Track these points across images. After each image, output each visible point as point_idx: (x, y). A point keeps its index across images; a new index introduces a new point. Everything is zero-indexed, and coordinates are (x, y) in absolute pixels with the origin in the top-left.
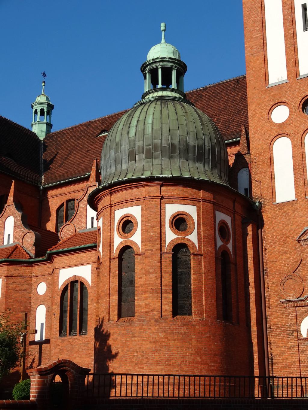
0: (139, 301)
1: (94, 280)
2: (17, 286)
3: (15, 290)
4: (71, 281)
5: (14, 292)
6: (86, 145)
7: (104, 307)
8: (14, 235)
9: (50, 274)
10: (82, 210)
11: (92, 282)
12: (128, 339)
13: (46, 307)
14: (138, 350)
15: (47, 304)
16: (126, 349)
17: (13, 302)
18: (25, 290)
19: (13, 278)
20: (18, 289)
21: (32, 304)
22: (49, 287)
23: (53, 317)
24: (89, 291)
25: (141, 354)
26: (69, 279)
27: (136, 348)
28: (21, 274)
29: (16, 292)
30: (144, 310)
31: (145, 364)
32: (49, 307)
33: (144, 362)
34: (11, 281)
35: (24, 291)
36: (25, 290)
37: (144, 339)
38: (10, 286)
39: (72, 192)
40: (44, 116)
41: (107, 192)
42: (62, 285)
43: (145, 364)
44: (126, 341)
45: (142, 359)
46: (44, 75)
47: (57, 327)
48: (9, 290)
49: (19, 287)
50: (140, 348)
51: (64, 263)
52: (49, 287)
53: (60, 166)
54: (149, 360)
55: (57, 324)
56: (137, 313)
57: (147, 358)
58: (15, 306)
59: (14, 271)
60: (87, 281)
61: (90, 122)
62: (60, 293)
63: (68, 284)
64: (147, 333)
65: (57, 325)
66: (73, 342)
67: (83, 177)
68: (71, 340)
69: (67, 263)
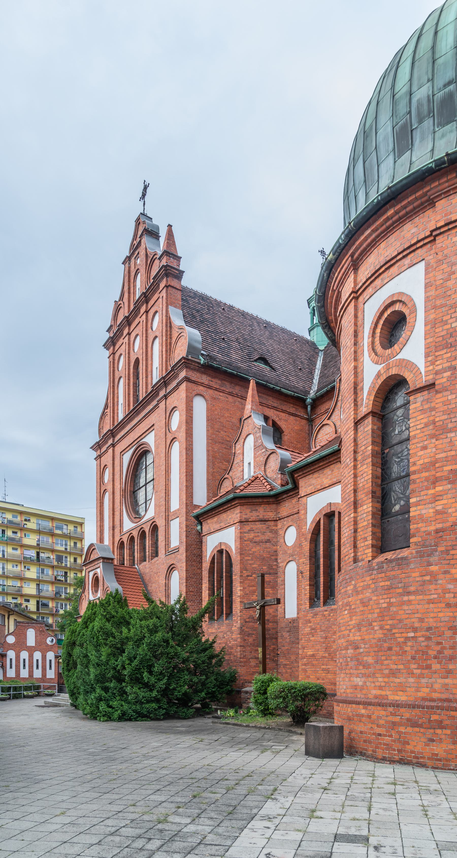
0: (419, 507)
2: (257, 534)
3: (254, 541)
4: (324, 513)
7: (347, 534)
12: (393, 600)
14: (416, 625)
16: (390, 622)
17: (252, 559)
18: (268, 540)
19: (250, 523)
21: (279, 561)
25: (423, 636)
27: (413, 620)
28: (261, 517)
29: (255, 544)
30: (432, 528)
31: (435, 657)
33: (432, 653)
34: (247, 528)
35: (266, 542)
36: (268, 541)
37: (432, 597)
38: (245, 537)
42: (312, 522)
43: (435, 657)
44: (390, 604)
45: (428, 647)
48: (245, 542)
50: (421, 620)
51: (314, 484)
54: (444, 648)
56: (414, 536)
57: (441, 643)
58: (254, 566)
59: (250, 512)
62: (309, 536)
64: (440, 582)
69: (318, 485)
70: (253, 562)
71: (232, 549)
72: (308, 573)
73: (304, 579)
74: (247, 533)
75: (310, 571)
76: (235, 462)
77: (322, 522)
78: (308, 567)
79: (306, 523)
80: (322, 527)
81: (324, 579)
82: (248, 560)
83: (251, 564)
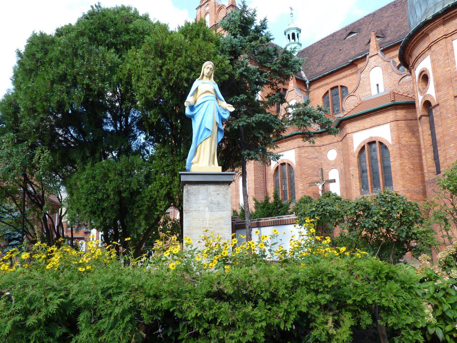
1: (395, 138)
7: (453, 153)
10: (365, 80)
11: (392, 141)
17: (307, 168)
19: (305, 148)
20: (310, 157)
23: (352, 177)
24: (390, 149)
34: (303, 150)
36: (316, 158)
39: (335, 81)
41: (438, 23)
46: (291, 9)
49: (310, 155)
53: (318, 66)
60: (386, 141)
62: (357, 155)
65: (356, 185)
67: (345, 65)
75: (359, 174)
78: (357, 172)
79: (353, 148)
83: (307, 171)
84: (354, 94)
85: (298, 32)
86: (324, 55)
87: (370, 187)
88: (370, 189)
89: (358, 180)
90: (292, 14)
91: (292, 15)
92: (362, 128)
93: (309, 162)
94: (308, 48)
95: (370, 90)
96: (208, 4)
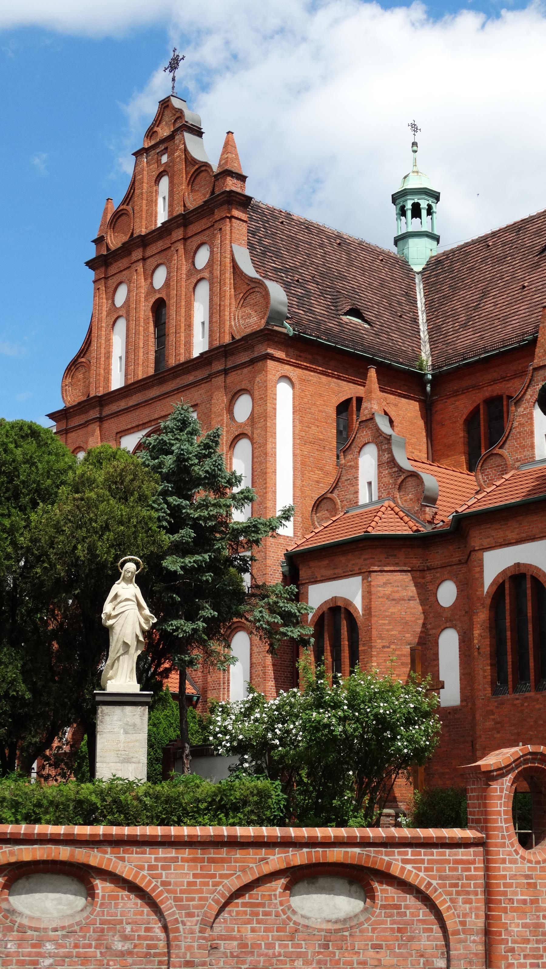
4: (509, 574)
5: (389, 602)
6: (519, 274)
8: (379, 482)
9: (463, 561)
10: (523, 420)
13: (458, 632)
15: (460, 625)
17: (389, 624)
18: (411, 597)
20: (396, 596)
22: (462, 591)
26: (504, 571)
29: (394, 602)
32: (465, 633)
35: (409, 600)
40: (421, 218)
42: (492, 585)
46: (414, 128)
47: (486, 674)
49: (397, 592)
51: (493, 536)
52: (462, 591)
53: (464, 326)
55: (485, 668)
58: (392, 633)
59: (386, 558)
61: (524, 223)
62: (488, 601)
63: (503, 584)
65: (485, 671)
66: (522, 705)
68: (518, 702)
69: (499, 538)
70: (391, 627)
71: (356, 608)
72: (488, 649)
73: (482, 656)
74: (382, 587)
75: (491, 646)
76: (344, 478)
77: (507, 586)
80: (507, 592)
81: (512, 658)
82: (384, 624)
84: (500, 451)
85: (431, 201)
86: (485, 294)
87: (510, 677)
88: (510, 683)
89: (489, 662)
90: (414, 144)
91: (415, 148)
92: (501, 540)
93: (394, 609)
94: (453, 251)
95: (532, 447)
96: (166, 149)
